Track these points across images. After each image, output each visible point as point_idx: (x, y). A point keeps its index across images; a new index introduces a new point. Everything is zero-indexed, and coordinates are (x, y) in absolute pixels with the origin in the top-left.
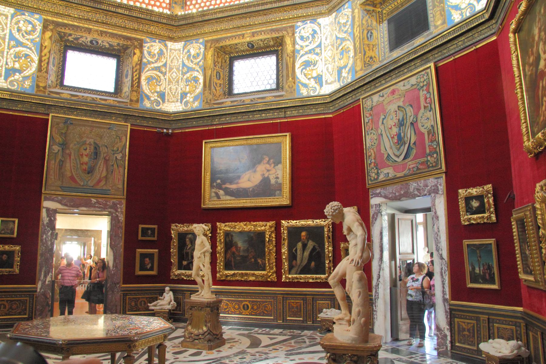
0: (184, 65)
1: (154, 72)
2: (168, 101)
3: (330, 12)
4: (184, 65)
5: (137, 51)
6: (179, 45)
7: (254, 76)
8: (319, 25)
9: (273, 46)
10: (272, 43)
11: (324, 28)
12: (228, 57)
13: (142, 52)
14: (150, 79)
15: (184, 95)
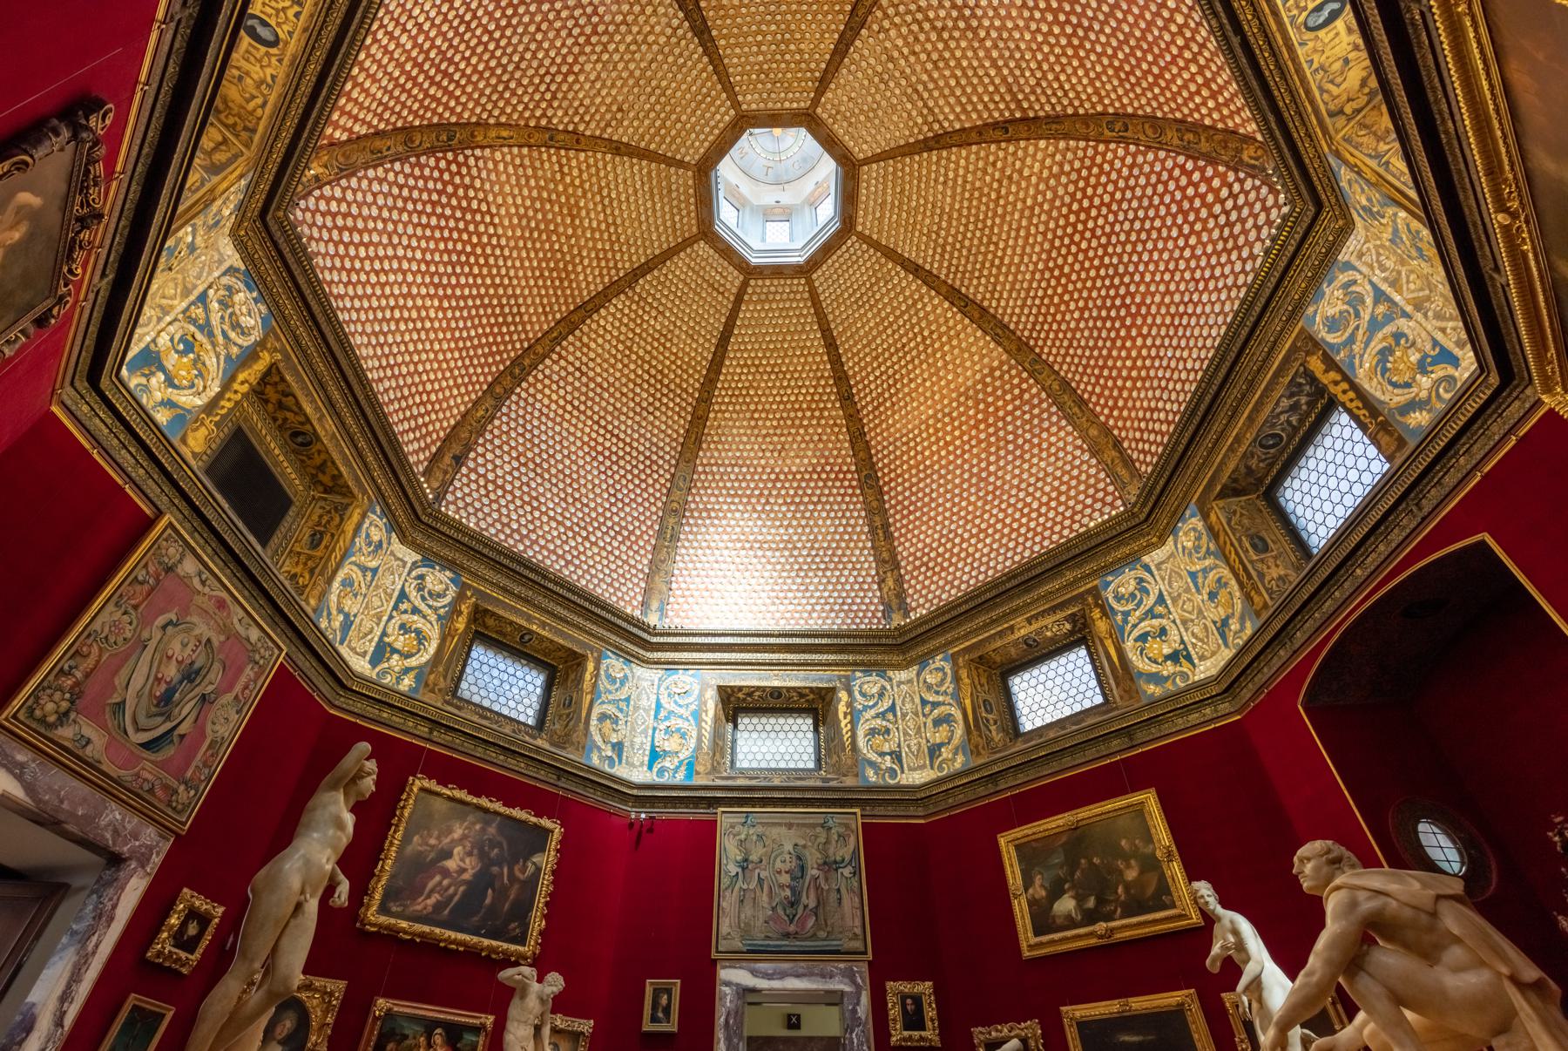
0: (924, 702)
1: (879, 721)
2: (910, 769)
3: (1162, 541)
4: (924, 702)
5: (843, 695)
6: (911, 673)
7: (1053, 693)
8: (1147, 568)
9: (1072, 633)
10: (1068, 626)
11: (1159, 569)
12: (997, 673)
13: (850, 694)
14: (872, 732)
15: (934, 751)
